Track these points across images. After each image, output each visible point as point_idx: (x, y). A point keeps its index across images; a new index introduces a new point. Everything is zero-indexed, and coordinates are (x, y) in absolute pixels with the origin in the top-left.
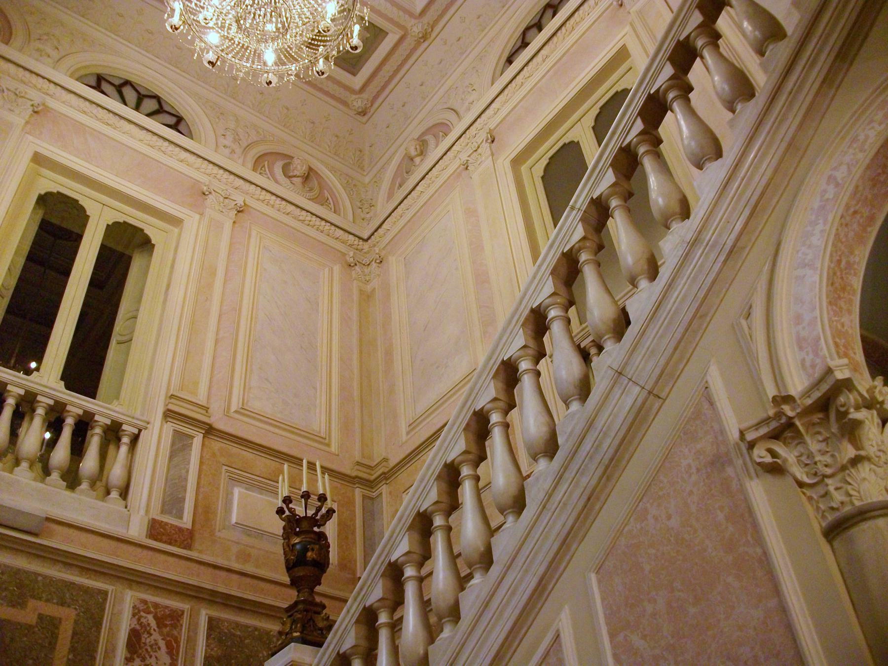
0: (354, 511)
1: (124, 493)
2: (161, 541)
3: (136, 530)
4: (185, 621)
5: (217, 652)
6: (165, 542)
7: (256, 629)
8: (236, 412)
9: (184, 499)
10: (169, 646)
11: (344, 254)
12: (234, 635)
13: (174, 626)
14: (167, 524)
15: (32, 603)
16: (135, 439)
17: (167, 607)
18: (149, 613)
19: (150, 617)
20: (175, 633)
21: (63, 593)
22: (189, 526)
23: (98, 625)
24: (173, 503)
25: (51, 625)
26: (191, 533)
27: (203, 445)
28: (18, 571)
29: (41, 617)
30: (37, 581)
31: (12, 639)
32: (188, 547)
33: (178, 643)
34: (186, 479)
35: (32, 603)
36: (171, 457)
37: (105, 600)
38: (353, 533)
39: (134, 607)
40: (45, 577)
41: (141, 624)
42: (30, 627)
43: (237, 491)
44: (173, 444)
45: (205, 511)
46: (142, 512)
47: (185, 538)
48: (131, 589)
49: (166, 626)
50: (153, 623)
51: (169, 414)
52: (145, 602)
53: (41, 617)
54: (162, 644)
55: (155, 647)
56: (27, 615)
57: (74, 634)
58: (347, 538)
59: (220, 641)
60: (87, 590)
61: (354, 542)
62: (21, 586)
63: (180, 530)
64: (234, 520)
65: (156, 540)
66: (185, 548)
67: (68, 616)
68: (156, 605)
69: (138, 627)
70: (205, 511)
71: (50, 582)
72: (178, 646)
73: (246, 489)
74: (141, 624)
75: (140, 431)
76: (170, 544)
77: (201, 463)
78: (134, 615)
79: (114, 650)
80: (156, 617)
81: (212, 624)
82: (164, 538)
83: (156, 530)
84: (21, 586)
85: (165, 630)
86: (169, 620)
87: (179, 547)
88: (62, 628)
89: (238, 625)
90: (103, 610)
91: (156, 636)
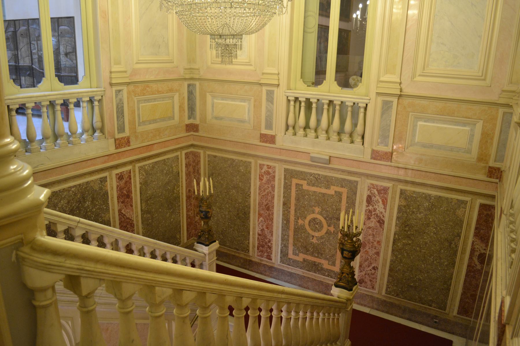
2: (377, 159)
4: (390, 192)
5: (404, 203)
6: (379, 160)
7: (423, 193)
10: (383, 201)
12: (412, 196)
13: (385, 193)
15: (332, 187)
16: (366, 109)
17: (382, 186)
18: (375, 188)
19: (375, 190)
20: (385, 196)
21: (342, 183)
23: (355, 194)
25: (339, 194)
28: (326, 176)
29: (335, 192)
30: (332, 180)
31: (328, 200)
33: (386, 199)
34: (390, 125)
35: (332, 187)
37: (357, 184)
38: (492, 139)
39: (368, 187)
40: (335, 178)
41: (371, 193)
42: (333, 195)
44: (383, 108)
48: (368, 179)
49: (382, 193)
50: (376, 193)
52: (373, 185)
53: (335, 192)
54: (380, 200)
55: (378, 202)
56: (331, 191)
57: (347, 197)
58: (487, 142)
59: (405, 199)
60: (350, 181)
61: (492, 144)
62: (328, 181)
65: (375, 159)
67: (344, 191)
68: (377, 186)
69: (370, 194)
71: (337, 179)
72: (387, 201)
74: (371, 193)
75: (367, 105)
78: (368, 190)
79: (363, 202)
80: (377, 190)
81: (402, 192)
82: (379, 158)
84: (328, 181)
85: (381, 195)
86: (383, 191)
88: (343, 195)
89: (414, 192)
90: (357, 188)
91: (378, 197)
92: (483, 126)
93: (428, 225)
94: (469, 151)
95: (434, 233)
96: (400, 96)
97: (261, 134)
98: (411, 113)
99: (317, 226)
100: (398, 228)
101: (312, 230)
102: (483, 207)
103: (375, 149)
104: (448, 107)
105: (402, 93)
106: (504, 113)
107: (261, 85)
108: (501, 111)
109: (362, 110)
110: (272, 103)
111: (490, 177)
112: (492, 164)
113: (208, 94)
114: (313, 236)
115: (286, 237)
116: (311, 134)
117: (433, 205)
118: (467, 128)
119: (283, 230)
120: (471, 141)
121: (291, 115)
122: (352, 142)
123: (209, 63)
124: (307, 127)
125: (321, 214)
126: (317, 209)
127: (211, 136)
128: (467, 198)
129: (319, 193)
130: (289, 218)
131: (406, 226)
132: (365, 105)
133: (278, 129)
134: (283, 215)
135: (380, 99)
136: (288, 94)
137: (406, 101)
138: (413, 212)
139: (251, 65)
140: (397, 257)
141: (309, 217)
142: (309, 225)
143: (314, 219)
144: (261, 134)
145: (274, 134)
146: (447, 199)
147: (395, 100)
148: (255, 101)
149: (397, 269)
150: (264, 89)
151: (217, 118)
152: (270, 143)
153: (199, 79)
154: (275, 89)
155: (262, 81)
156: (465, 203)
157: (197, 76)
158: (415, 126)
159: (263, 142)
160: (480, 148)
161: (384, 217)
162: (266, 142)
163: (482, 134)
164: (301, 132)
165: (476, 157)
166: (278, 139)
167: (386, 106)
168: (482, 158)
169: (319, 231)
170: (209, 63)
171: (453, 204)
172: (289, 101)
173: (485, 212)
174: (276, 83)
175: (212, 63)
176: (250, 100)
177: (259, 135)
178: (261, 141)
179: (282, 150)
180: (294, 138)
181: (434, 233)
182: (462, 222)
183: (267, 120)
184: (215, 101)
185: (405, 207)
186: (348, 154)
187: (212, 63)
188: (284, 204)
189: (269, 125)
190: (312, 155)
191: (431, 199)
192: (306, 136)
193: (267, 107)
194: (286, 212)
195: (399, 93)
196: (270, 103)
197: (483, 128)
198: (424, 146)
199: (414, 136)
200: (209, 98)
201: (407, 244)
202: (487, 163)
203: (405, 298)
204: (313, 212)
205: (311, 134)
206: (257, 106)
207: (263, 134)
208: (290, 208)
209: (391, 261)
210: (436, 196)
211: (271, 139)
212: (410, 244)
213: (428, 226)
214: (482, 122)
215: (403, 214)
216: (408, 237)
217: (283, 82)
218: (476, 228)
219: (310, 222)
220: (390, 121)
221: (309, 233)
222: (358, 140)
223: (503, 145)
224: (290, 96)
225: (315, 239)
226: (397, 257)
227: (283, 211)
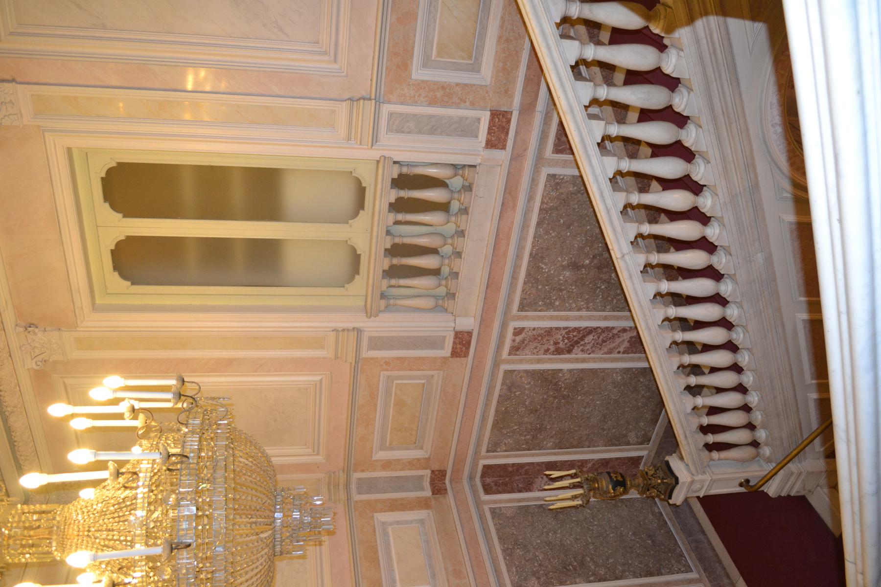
0: (377, 501)
7: (505, 559)
12: (517, 571)
38: (395, 500)
58: (401, 504)
59: (526, 580)
89: (508, 571)
93: (549, 543)
94: (422, 522)
95: (555, 533)
100: (577, 580)
102: (488, 490)
111: (446, 490)
112: (428, 493)
117: (516, 544)
118: (390, 530)
128: (486, 508)
131: (569, 570)
138: (540, 565)
140: (624, 571)
146: (498, 530)
149: (642, 566)
156: (493, 511)
160: (411, 509)
163: (393, 511)
165: (426, 511)
168: (424, 504)
171: (501, 522)
173: (494, 488)
181: (555, 533)
182: (520, 508)
185: (538, 578)
191: (508, 549)
201: (594, 562)
202: (429, 498)
203: (676, 543)
209: (635, 576)
210: (500, 543)
212: (592, 559)
213: (550, 543)
214: (375, 515)
215: (552, 578)
216: (582, 563)
218: (520, 491)
223: (398, 484)
226: (624, 571)
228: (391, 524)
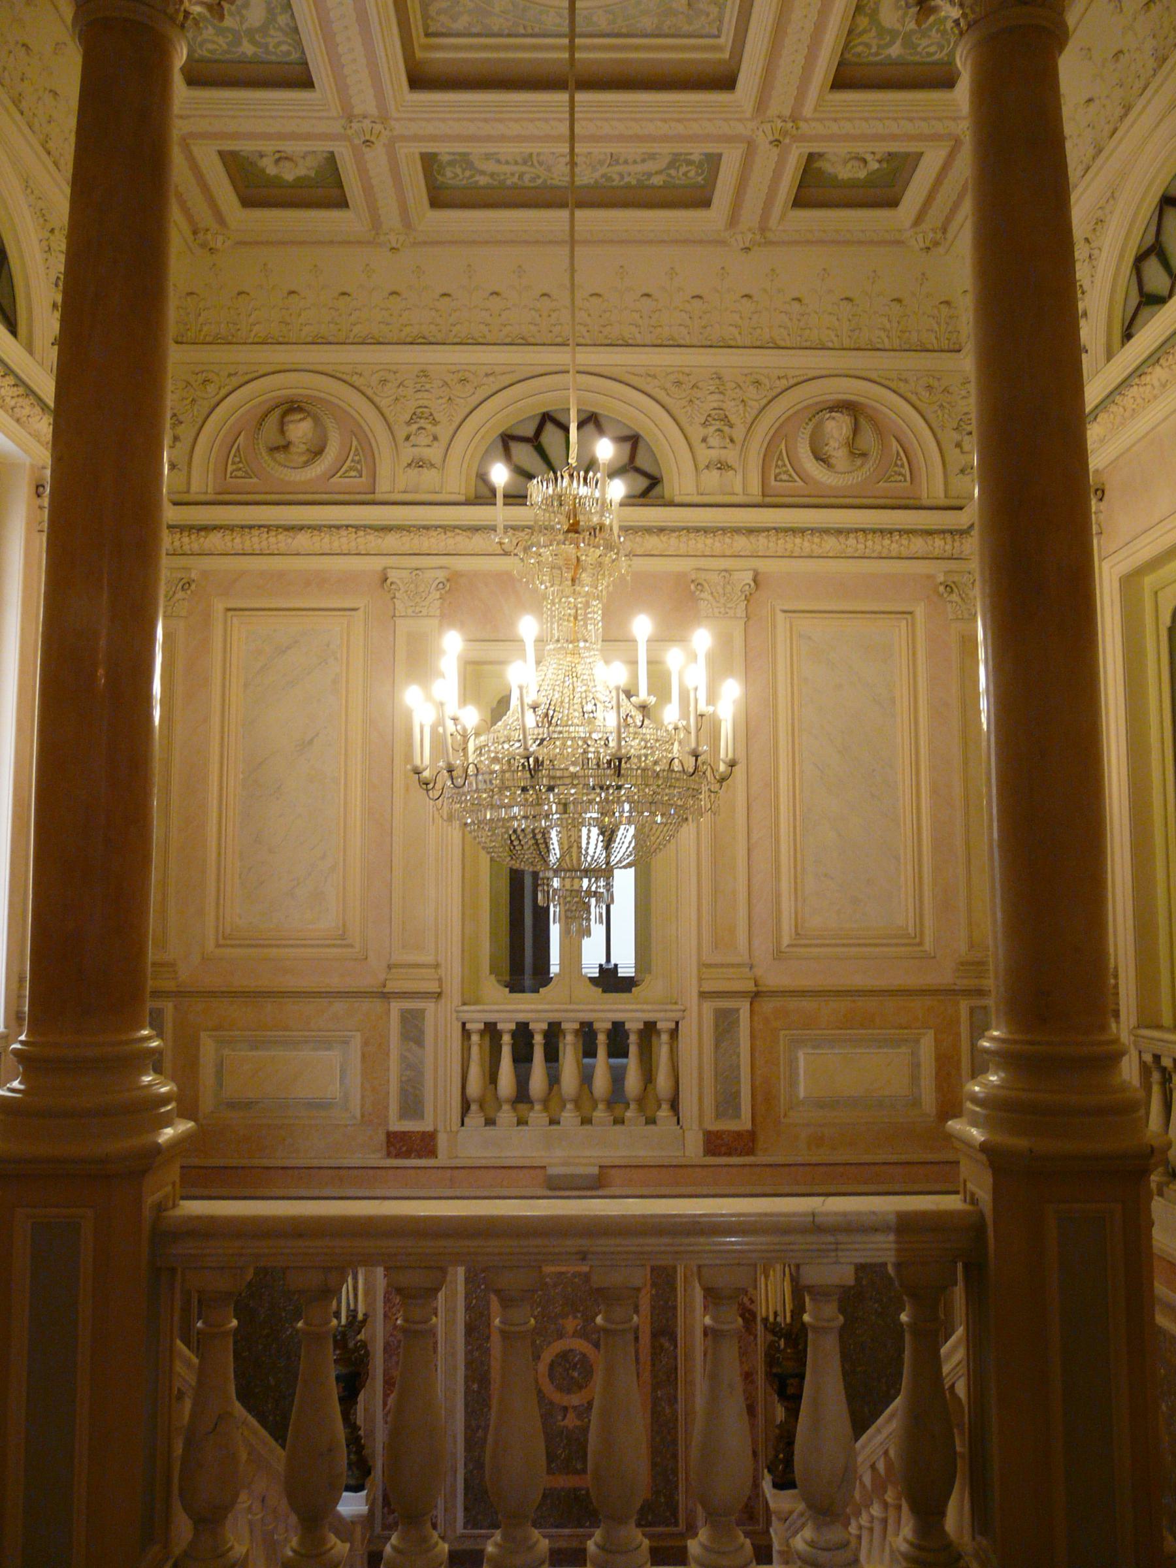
0: (958, 1035)
1: (674, 1105)
2: (720, 1155)
3: (693, 1148)
6: (725, 1154)
8: (788, 946)
9: (738, 1093)
11: (930, 577)
14: (724, 1132)
16: (674, 1033)
22: (749, 1126)
24: (727, 1103)
26: (752, 1135)
27: (752, 1012)
32: (751, 1152)
34: (738, 1066)
36: (716, 1052)
43: (801, 1055)
44: (717, 1026)
45: (764, 1098)
46: (695, 1127)
47: (744, 1143)
51: (703, 995)
63: (739, 1135)
64: (802, 1094)
65: (714, 1155)
66: (748, 1154)
70: (764, 1098)
73: (814, 1047)
75: (677, 1023)
76: (729, 1154)
77: (753, 1037)
83: (715, 1144)
87: (740, 1155)
92: (936, 1040)
94: (916, 1103)
96: (756, 996)
97: (389, 1135)
98: (782, 1033)
99: (576, 1374)
101: (560, 1388)
103: (710, 1128)
104: (860, 1011)
105: (760, 989)
106: (972, 1010)
107: (385, 996)
108: (964, 1005)
109: (665, 1037)
110: (420, 1042)
113: (203, 1035)
114: (565, 1409)
115: (480, 1433)
116: (538, 1116)
119: (470, 1413)
120: (915, 1079)
121: (475, 1071)
122: (651, 1121)
123: (210, 945)
124: (522, 1095)
125: (582, 1334)
126: (570, 1324)
127: (221, 1162)
129: (574, 1275)
130: (488, 1371)
132: (673, 1025)
133: (439, 1112)
134: (468, 1365)
135: (708, 1007)
136: (465, 1017)
137: (767, 1006)
139: (352, 946)
141: (547, 1356)
142: (551, 1376)
143: (564, 1355)
144: (389, 1135)
145: (430, 1128)
147: (744, 1007)
148: (366, 1043)
150: (396, 1006)
151: (232, 1105)
152: (420, 1157)
153: (178, 994)
154: (429, 1006)
155: (391, 987)
157: (170, 985)
158: (792, 1063)
159: (397, 1156)
160: (939, 1088)
161: (752, 1302)
162: (407, 1155)
163: (937, 1059)
164: (506, 1115)
166: (442, 1141)
167: (725, 1023)
169: (581, 1388)
170: (210, 945)
172: (466, 1033)
174: (433, 987)
175: (218, 946)
176: (347, 1043)
177: (383, 1138)
178: (389, 1155)
179: (456, 1172)
180: (490, 1131)
183: (403, 1092)
184: (226, 1052)
186: (644, 1153)
187: (218, 946)
188: (470, 1329)
189: (412, 1105)
190: (551, 1171)
192: (522, 1122)
193: (403, 1058)
194: (476, 1354)
195: (754, 989)
196: (412, 1044)
197: (936, 1047)
198: (820, 1104)
199: (793, 1083)
200: (208, 1048)
204: (561, 1336)
205: (538, 1116)
206: (374, 1058)
207: (395, 1134)
208: (488, 1338)
211: (425, 1144)
214: (932, 1032)
217: (454, 988)
219: (552, 1366)
220: (739, 1057)
221: (551, 1403)
222: (664, 1113)
224: (472, 1021)
225: (571, 1415)
227: (468, 1353)
228: (913, 1054)
